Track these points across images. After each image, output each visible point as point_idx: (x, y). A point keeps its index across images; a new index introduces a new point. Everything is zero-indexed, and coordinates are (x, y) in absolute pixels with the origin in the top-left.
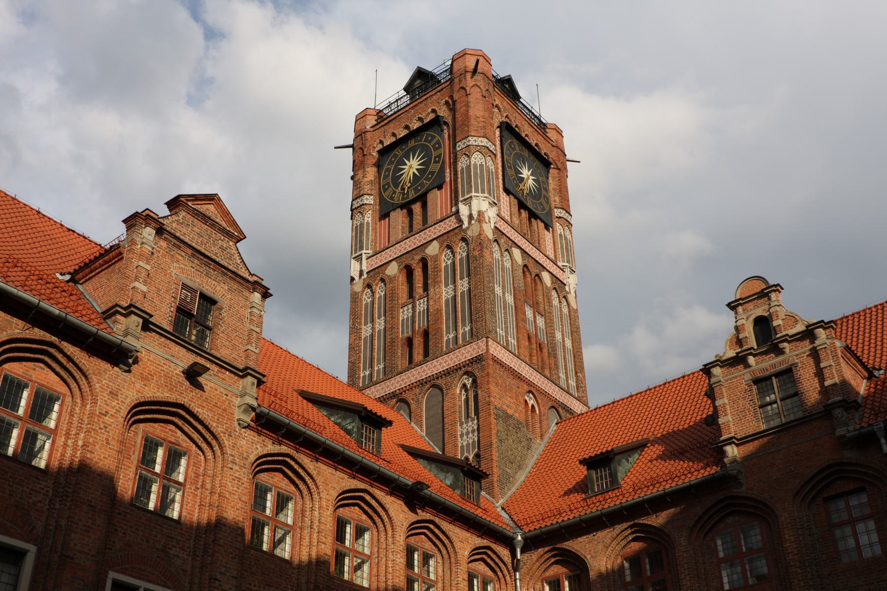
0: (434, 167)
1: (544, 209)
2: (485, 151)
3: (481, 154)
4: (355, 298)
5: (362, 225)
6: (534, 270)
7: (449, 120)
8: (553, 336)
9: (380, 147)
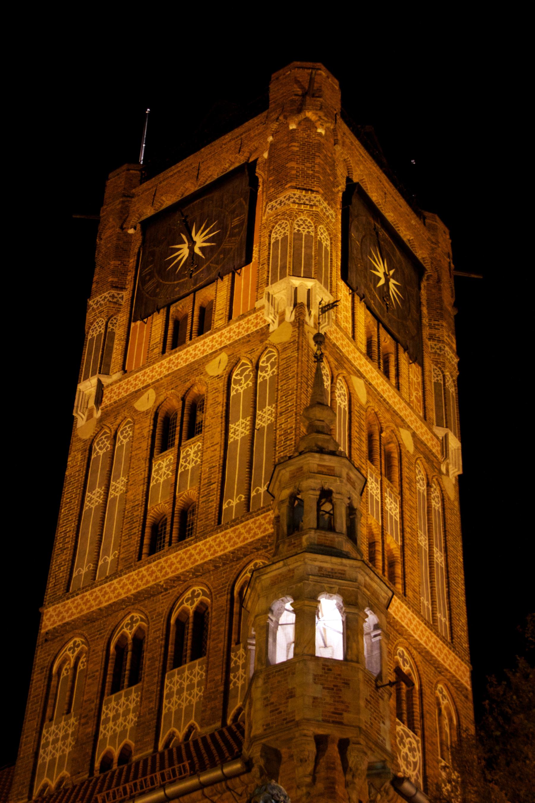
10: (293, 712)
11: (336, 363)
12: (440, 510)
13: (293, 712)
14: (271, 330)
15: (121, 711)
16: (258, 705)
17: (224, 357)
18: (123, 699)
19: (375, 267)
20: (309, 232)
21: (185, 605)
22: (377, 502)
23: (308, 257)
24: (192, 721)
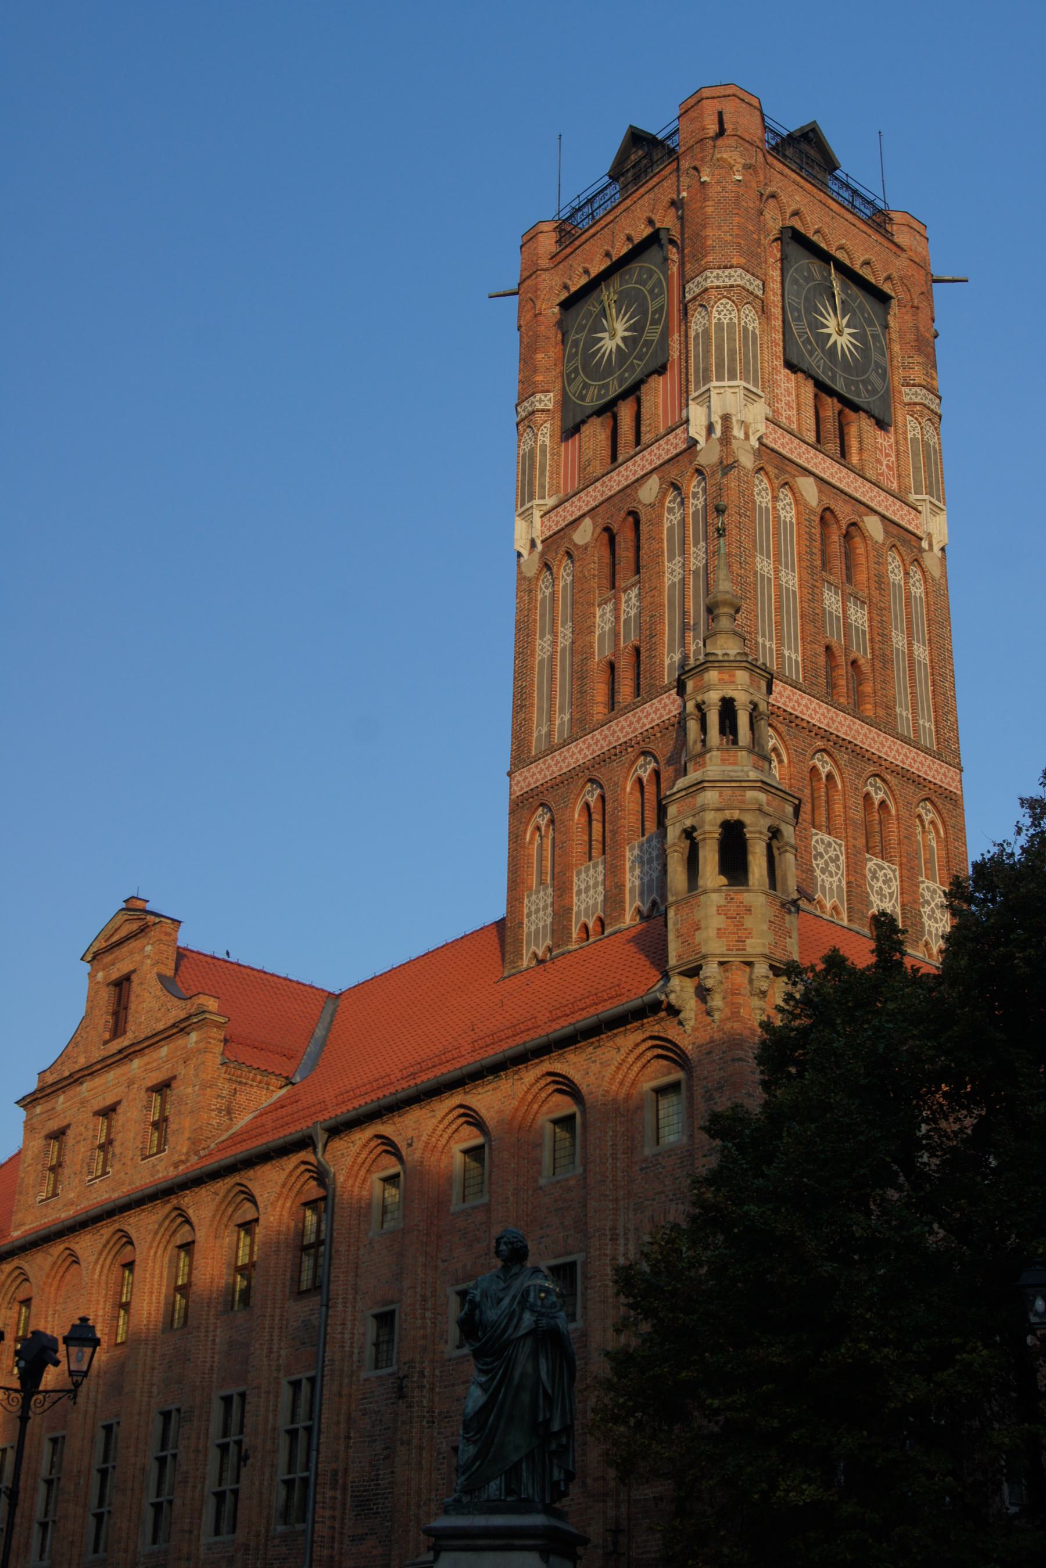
0: (652, 333)
1: (874, 392)
2: (740, 296)
3: (732, 305)
4: (526, 586)
5: (532, 451)
6: (845, 513)
7: (676, 234)
8: (886, 638)
9: (564, 295)
10: (699, 945)
11: (777, 471)
12: (923, 596)
13: (699, 945)
14: (699, 447)
15: (591, 883)
16: (671, 936)
17: (654, 482)
18: (592, 871)
19: (822, 323)
20: (731, 319)
21: (639, 772)
22: (838, 618)
23: (732, 352)
24: (654, 895)
